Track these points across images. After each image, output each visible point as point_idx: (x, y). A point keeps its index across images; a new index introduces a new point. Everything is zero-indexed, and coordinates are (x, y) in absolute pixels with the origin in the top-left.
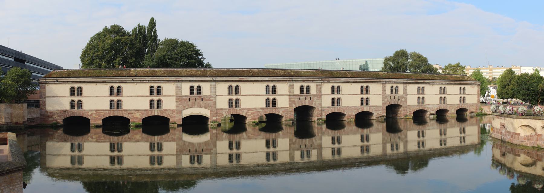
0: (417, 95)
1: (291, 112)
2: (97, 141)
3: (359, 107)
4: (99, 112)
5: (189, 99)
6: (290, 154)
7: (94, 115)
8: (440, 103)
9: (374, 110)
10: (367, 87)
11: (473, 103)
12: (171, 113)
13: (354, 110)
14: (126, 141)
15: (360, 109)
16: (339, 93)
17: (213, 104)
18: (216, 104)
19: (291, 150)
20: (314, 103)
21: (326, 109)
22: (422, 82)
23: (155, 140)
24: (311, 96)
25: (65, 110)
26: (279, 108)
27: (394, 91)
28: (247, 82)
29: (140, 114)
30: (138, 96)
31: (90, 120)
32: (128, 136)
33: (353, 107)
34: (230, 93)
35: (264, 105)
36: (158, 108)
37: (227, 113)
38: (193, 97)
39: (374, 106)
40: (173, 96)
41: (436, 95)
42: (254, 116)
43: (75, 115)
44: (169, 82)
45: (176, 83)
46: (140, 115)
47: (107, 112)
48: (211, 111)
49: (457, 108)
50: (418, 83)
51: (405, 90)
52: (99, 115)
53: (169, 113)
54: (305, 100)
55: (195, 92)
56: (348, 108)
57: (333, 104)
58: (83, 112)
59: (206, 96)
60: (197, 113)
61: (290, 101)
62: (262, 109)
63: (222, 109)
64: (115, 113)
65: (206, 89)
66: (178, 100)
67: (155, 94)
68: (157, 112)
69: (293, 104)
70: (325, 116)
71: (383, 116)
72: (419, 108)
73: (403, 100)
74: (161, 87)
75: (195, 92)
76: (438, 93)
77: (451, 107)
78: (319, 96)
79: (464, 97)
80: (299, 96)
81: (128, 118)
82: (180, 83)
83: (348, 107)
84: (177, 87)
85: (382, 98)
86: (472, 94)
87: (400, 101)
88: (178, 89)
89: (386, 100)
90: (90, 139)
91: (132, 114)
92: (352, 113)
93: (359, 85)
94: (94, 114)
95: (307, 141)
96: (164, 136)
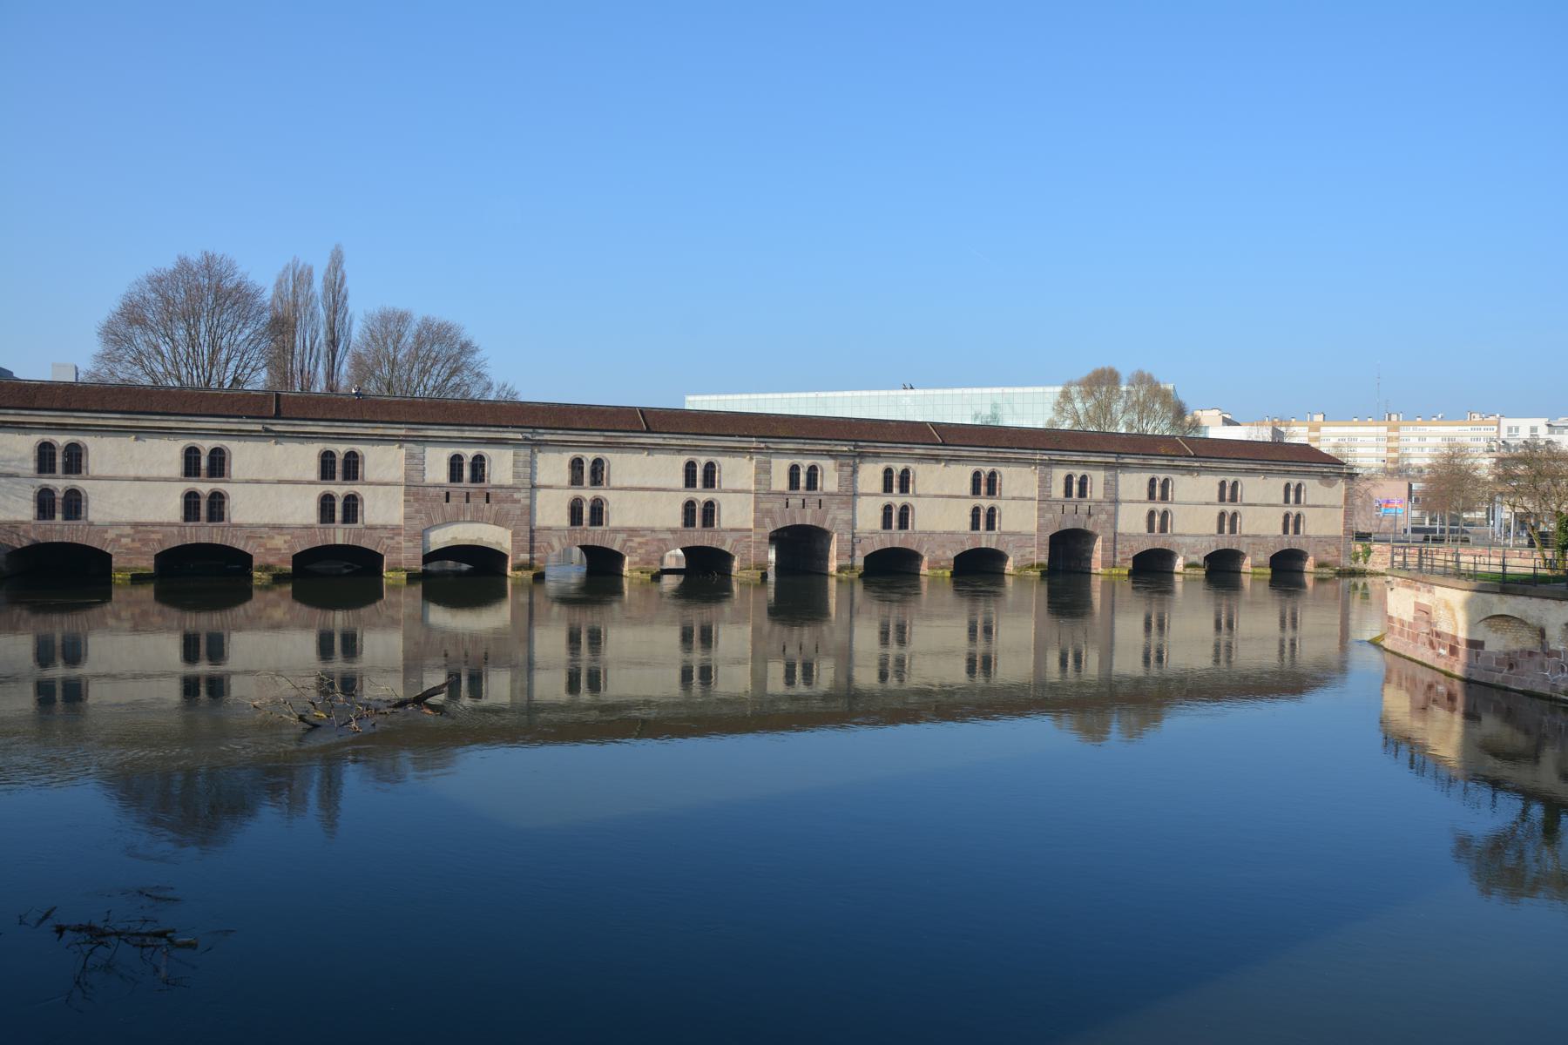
0: (1145, 502)
1: (761, 542)
2: (135, 629)
3: (965, 534)
4: (144, 531)
5: (448, 494)
6: (753, 672)
7: (124, 541)
8: (1221, 530)
9: (1011, 545)
10: (993, 475)
11: (1327, 534)
12: (387, 538)
14: (239, 629)
15: (970, 541)
16: (907, 491)
19: (759, 659)
20: (830, 517)
21: (867, 538)
22: (1165, 463)
23: (336, 623)
24: (821, 497)
25: (16, 522)
26: (723, 531)
27: (1075, 488)
30: (280, 482)
31: (109, 556)
32: (246, 611)
34: (576, 480)
35: (677, 521)
37: (564, 541)
38: (459, 490)
40: (396, 484)
41: (1207, 504)
42: (648, 553)
43: (54, 541)
45: (406, 445)
46: (285, 542)
48: (513, 535)
49: (1275, 547)
50: (1152, 467)
51: (1111, 487)
52: (145, 542)
53: (382, 538)
54: (804, 507)
55: (467, 473)
57: (887, 524)
58: (83, 531)
59: (501, 487)
60: (472, 540)
62: (673, 531)
63: (549, 529)
64: (204, 533)
65: (502, 466)
67: (339, 476)
68: (344, 534)
69: (767, 520)
70: (863, 559)
71: (1039, 565)
72: (1153, 544)
73: (1103, 517)
74: (359, 454)
75: (467, 473)
76: (1215, 497)
77: (1254, 544)
78: (845, 498)
79: (1298, 516)
81: (247, 550)
83: (932, 533)
84: (410, 456)
85: (1039, 509)
86: (1324, 506)
87: (1092, 519)
88: (415, 465)
90: (111, 622)
91: (261, 540)
92: (944, 553)
93: (967, 471)
94: (127, 536)
95: (806, 634)
96: (365, 612)
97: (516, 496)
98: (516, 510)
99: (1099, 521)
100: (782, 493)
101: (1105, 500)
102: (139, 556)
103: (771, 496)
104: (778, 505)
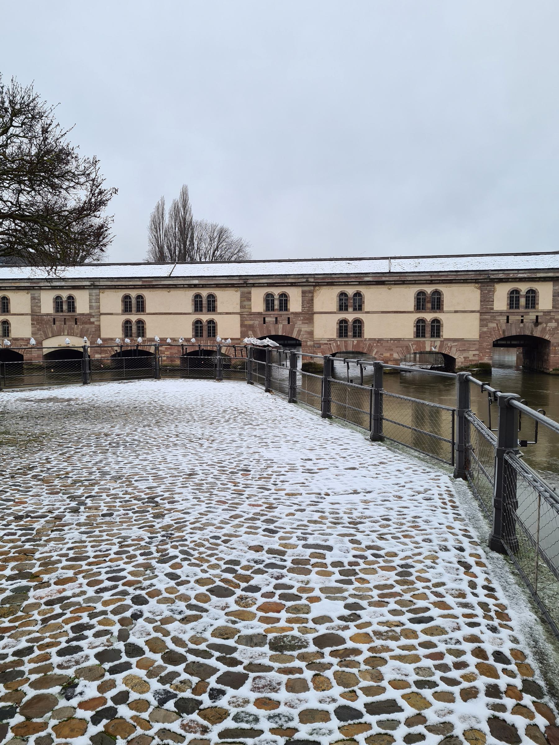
3: (410, 340)
9: (454, 349)
13: (397, 347)
15: (415, 346)
17: (96, 331)
18: (100, 330)
24: (290, 316)
28: (157, 289)
33: (395, 340)
39: (455, 340)
40: (27, 314)
56: (382, 342)
59: (83, 314)
61: (242, 325)
66: (35, 323)
75: (65, 307)
78: (307, 316)
80: (263, 316)
82: (38, 292)
83: (380, 341)
84: (33, 298)
85: (481, 320)
87: (540, 327)
92: (391, 355)
99: (548, 328)
100: (260, 314)
101: (555, 310)
103: (252, 316)
104: (257, 322)
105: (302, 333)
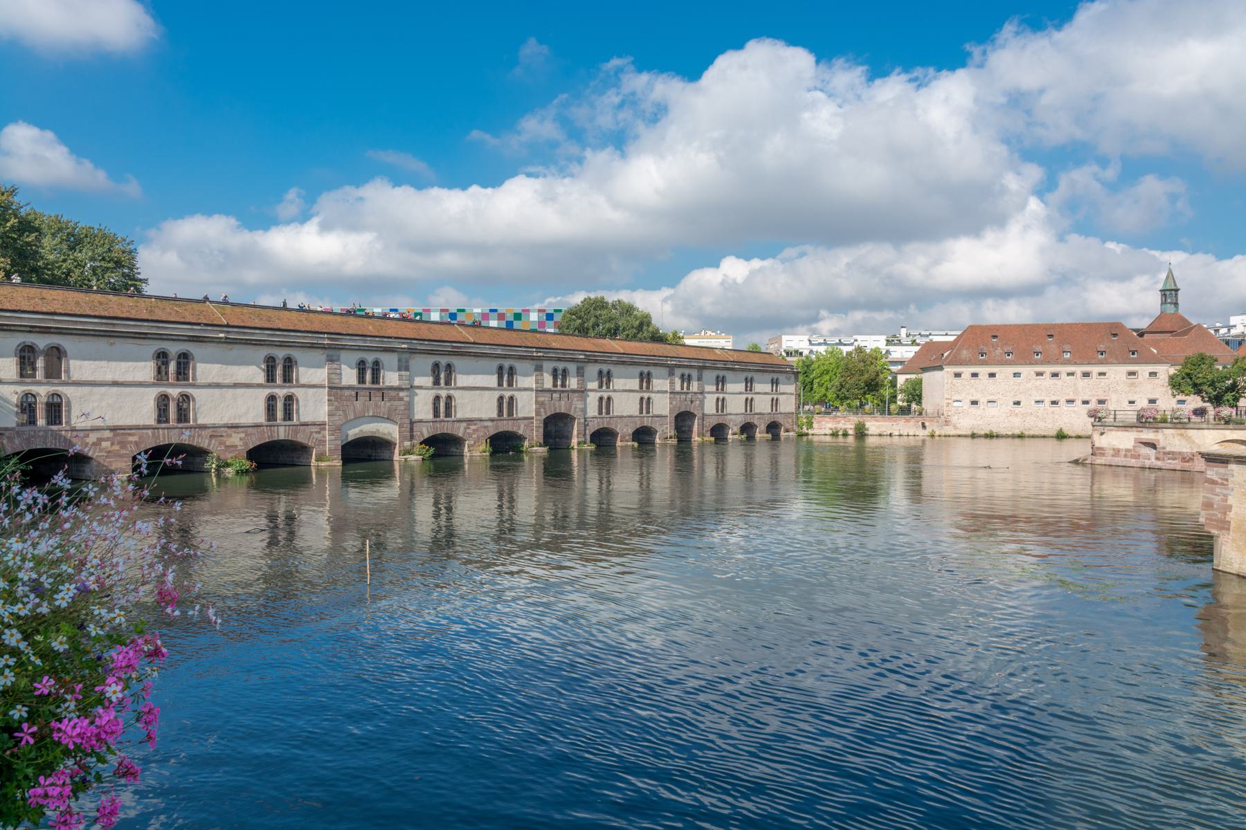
4: (122, 434)
7: (105, 444)
12: (316, 432)
20: (573, 407)
29: (243, 435)
30: (236, 386)
36: (285, 419)
42: (478, 438)
44: (312, 346)
46: (241, 439)
47: (147, 434)
62: (492, 420)
64: (173, 435)
66: (333, 398)
69: (542, 410)
73: (698, 402)
74: (293, 360)
83: (622, 417)
89: (674, 403)
94: (107, 439)
97: (402, 394)
98: (400, 406)
100: (549, 391)
102: (118, 459)
105: (578, 410)
